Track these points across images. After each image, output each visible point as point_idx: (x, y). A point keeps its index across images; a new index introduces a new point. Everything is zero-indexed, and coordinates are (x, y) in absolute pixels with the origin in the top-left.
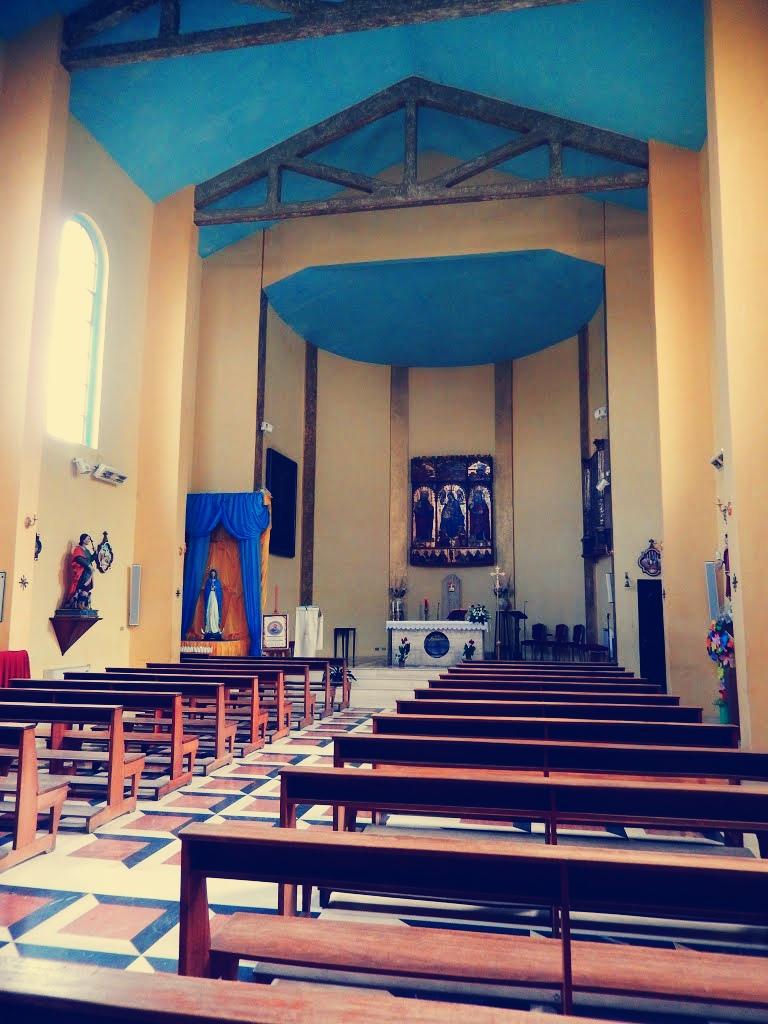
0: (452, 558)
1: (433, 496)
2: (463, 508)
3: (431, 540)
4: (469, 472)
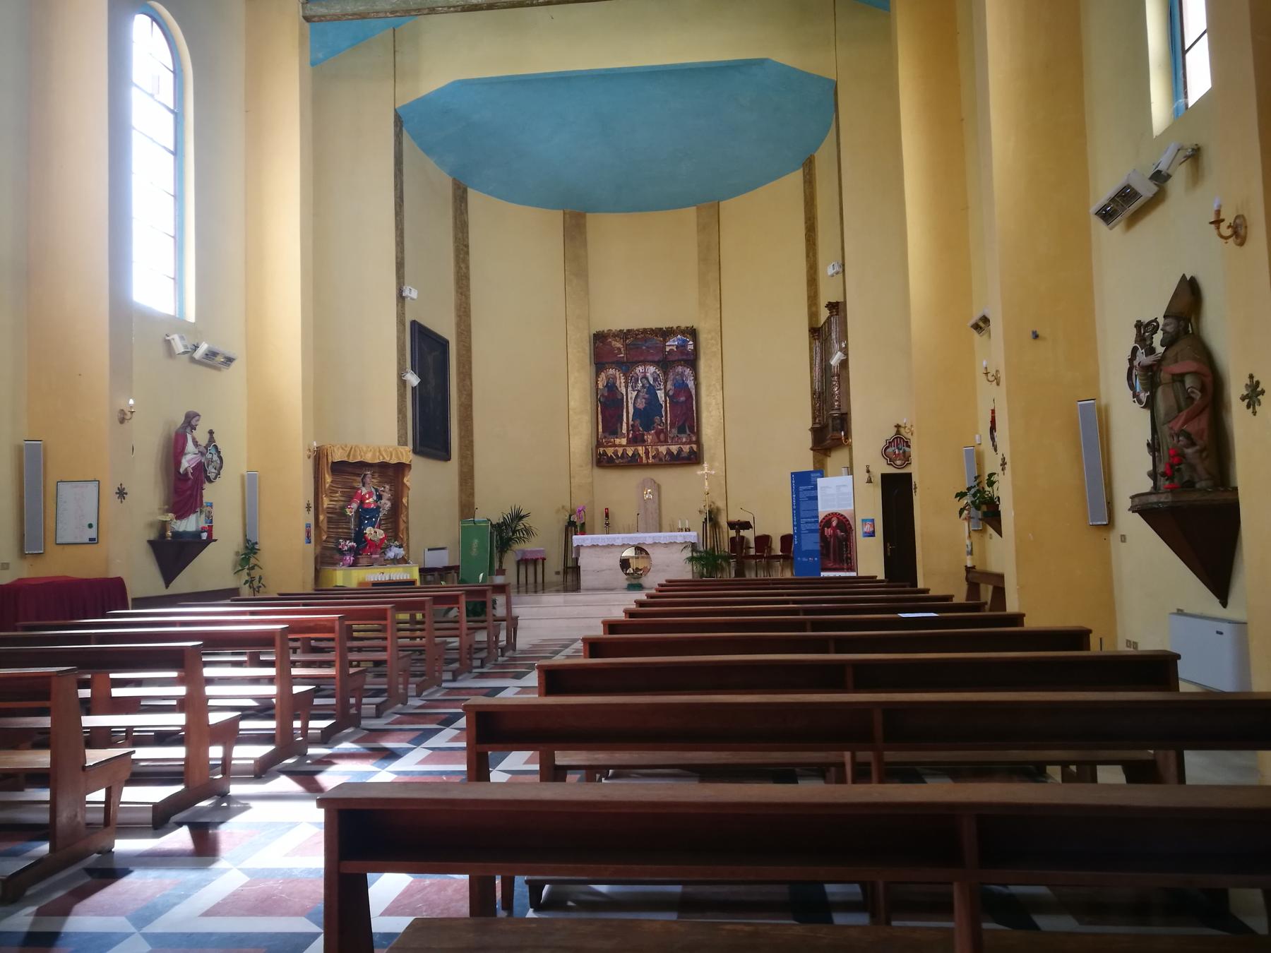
0: (647, 457)
1: (623, 381)
2: (661, 394)
3: (622, 436)
4: (668, 349)
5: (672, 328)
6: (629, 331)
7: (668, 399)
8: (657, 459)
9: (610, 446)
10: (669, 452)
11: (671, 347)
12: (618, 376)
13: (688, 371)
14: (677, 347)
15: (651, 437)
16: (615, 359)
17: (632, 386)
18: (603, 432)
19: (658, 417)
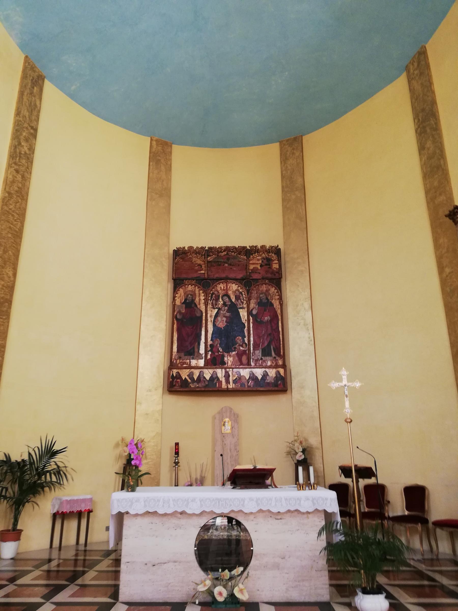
0: (228, 382)
1: (202, 298)
2: (243, 314)
3: (199, 357)
4: (251, 267)
5: (256, 247)
6: (210, 248)
7: (251, 318)
9: (186, 368)
10: (253, 377)
11: (254, 266)
12: (197, 292)
13: (273, 290)
14: (261, 266)
15: (231, 359)
16: (195, 275)
17: (212, 303)
18: (178, 351)
19: (240, 338)
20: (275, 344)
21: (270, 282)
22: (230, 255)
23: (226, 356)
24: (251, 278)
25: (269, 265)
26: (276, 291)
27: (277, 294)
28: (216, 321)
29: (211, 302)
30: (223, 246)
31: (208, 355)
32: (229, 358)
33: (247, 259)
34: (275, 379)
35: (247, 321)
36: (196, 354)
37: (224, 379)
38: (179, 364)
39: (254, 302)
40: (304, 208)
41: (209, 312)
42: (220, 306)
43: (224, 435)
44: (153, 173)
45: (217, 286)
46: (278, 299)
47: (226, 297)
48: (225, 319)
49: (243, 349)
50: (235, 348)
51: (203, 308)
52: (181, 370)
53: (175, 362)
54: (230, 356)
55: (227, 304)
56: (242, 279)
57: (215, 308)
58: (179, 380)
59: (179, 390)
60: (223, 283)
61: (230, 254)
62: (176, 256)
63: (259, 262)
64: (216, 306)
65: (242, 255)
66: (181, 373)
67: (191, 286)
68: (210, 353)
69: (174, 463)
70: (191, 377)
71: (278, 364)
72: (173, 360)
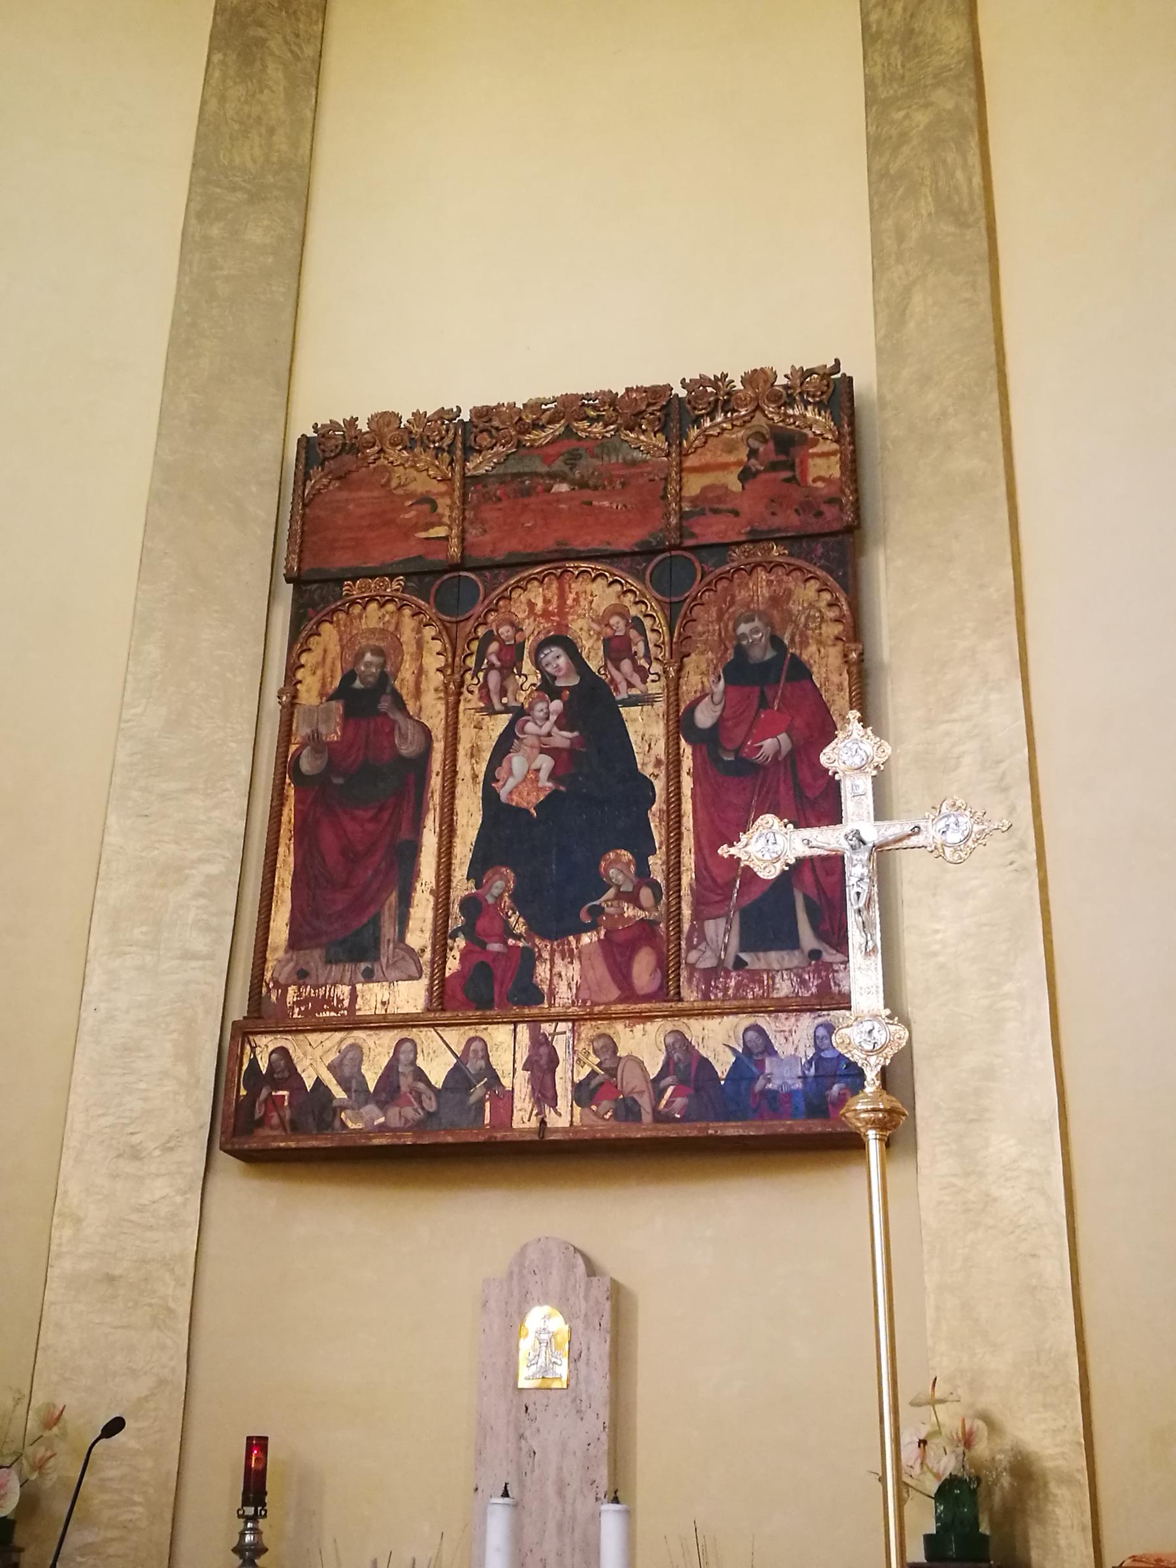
0: (544, 1094)
1: (433, 662)
4: (694, 485)
5: (716, 382)
6: (483, 414)
7: (686, 749)
8: (606, 1107)
12: (407, 635)
14: (746, 475)
15: (572, 971)
16: (403, 551)
18: (294, 943)
19: (626, 856)
20: (817, 881)
21: (791, 555)
22: (580, 438)
23: (546, 955)
24: (689, 542)
25: (792, 467)
26: (827, 596)
27: (832, 614)
28: (500, 773)
29: (476, 681)
30: (548, 395)
31: (450, 955)
32: (560, 965)
33: (670, 445)
34: (813, 1070)
35: (663, 767)
36: (387, 951)
37: (523, 1076)
38: (297, 1010)
39: (704, 666)
40: (974, 159)
41: (466, 735)
42: (522, 699)
43: (526, 1399)
44: (223, 99)
45: (510, 599)
46: (838, 638)
47: (556, 650)
48: (545, 763)
49: (641, 914)
50: (599, 910)
51: (433, 712)
52: (301, 1037)
53: (274, 998)
54: (569, 955)
55: (559, 683)
56: (646, 552)
57: (498, 707)
58: (285, 1093)
59: (282, 1144)
60: (542, 582)
61: (584, 430)
62: (308, 466)
63: (732, 458)
64: (505, 700)
65: (644, 432)
66: (296, 1055)
67: (382, 606)
68: (461, 942)
69: (235, 1550)
70: (347, 1071)
71: (835, 989)
72: (264, 990)
